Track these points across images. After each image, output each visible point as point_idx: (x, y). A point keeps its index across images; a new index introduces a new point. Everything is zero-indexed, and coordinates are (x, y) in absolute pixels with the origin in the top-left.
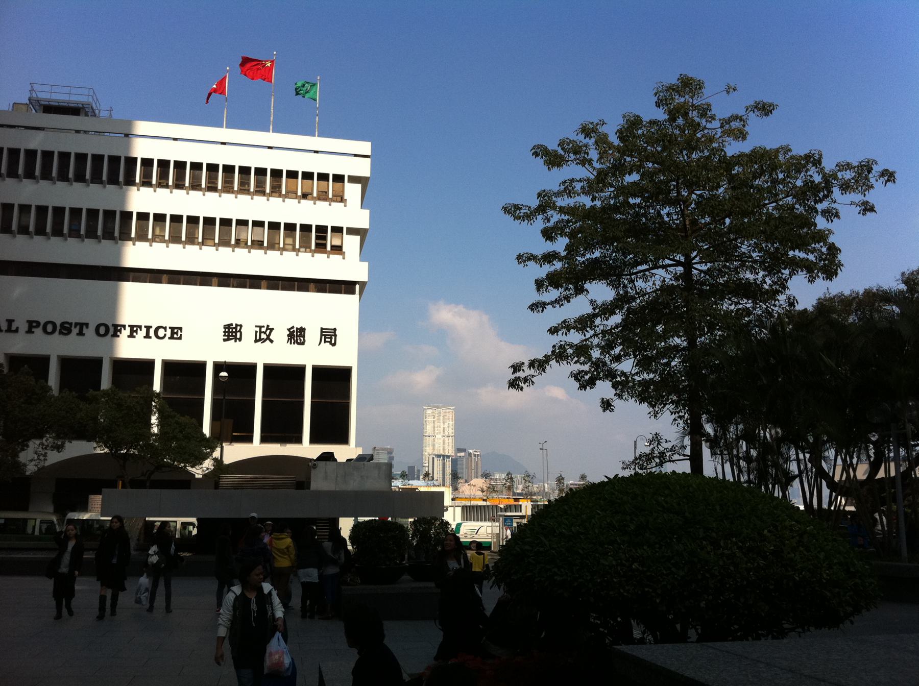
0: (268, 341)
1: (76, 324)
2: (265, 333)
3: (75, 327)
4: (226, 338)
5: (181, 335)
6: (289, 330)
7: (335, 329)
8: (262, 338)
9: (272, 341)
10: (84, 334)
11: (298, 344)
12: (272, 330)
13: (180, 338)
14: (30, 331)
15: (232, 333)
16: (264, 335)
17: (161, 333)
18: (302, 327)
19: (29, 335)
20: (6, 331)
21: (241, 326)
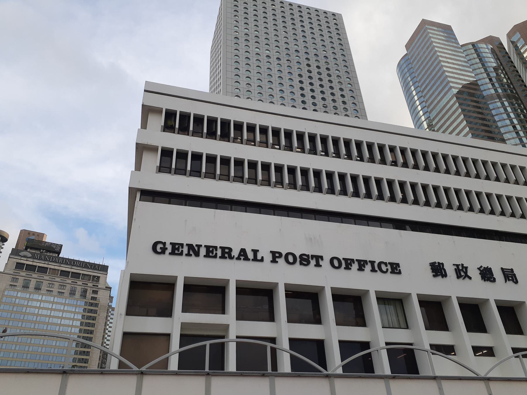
0: (467, 279)
1: (313, 257)
2: (462, 270)
3: (312, 259)
4: (434, 274)
5: (400, 270)
6: (479, 269)
8: (462, 275)
10: (321, 266)
11: (491, 281)
12: (466, 268)
13: (400, 273)
17: (384, 268)
18: (488, 267)
19: (274, 265)
20: (253, 260)
21: (443, 264)
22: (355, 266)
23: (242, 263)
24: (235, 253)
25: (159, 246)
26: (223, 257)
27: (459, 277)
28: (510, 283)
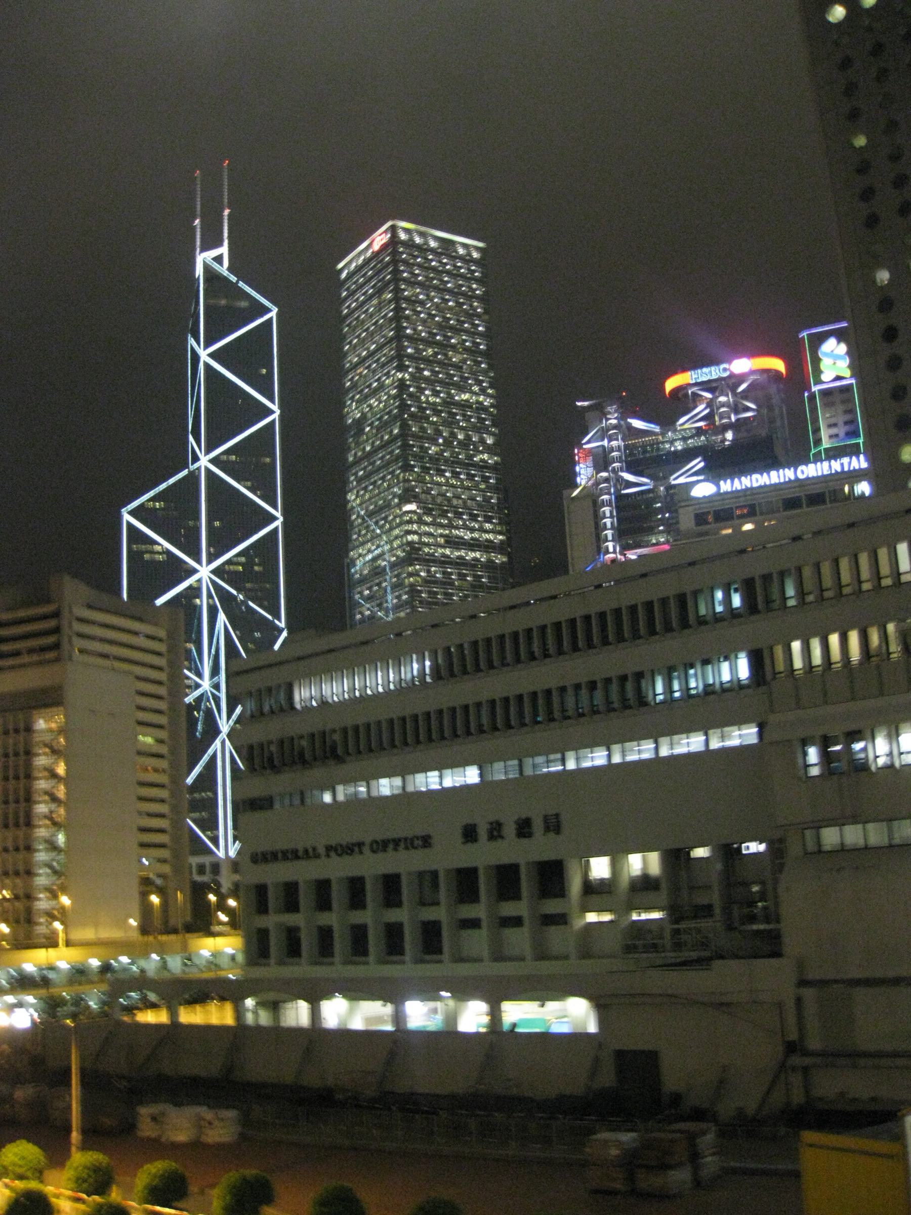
0: (500, 840)
7: (557, 815)
9: (502, 837)
14: (328, 856)
15: (470, 834)
16: (496, 831)
17: (416, 842)
22: (391, 846)
24: (300, 853)
28: (552, 835)
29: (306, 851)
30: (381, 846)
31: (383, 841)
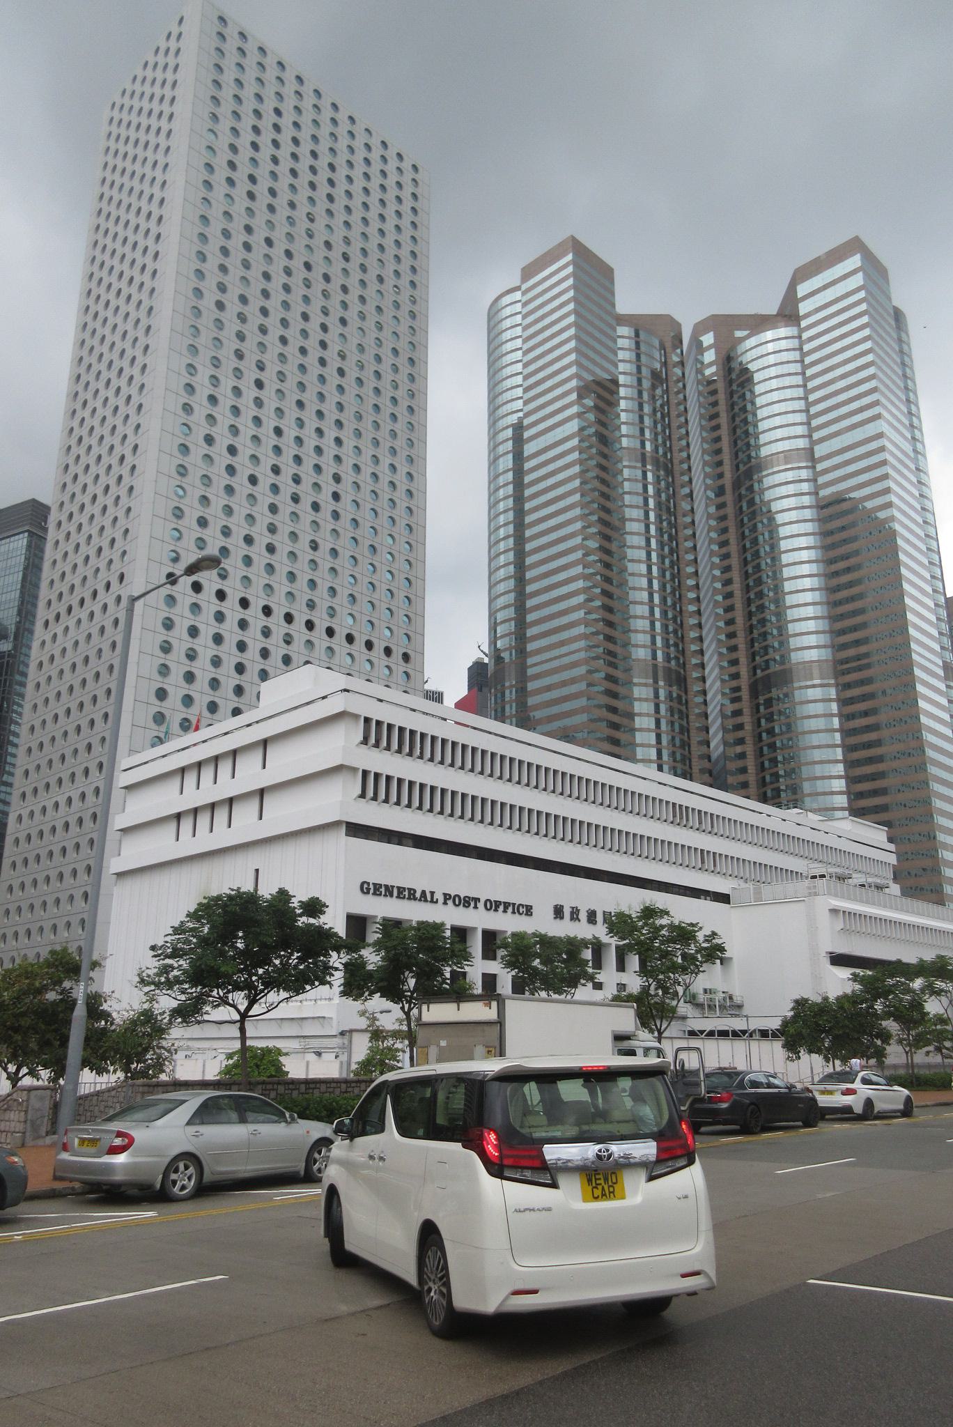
14: (445, 903)
17: (521, 910)
22: (501, 908)
23: (423, 904)
24: (418, 895)
25: (365, 886)
26: (409, 898)
27: (572, 919)
29: (424, 892)
30: (493, 906)
31: (495, 902)
